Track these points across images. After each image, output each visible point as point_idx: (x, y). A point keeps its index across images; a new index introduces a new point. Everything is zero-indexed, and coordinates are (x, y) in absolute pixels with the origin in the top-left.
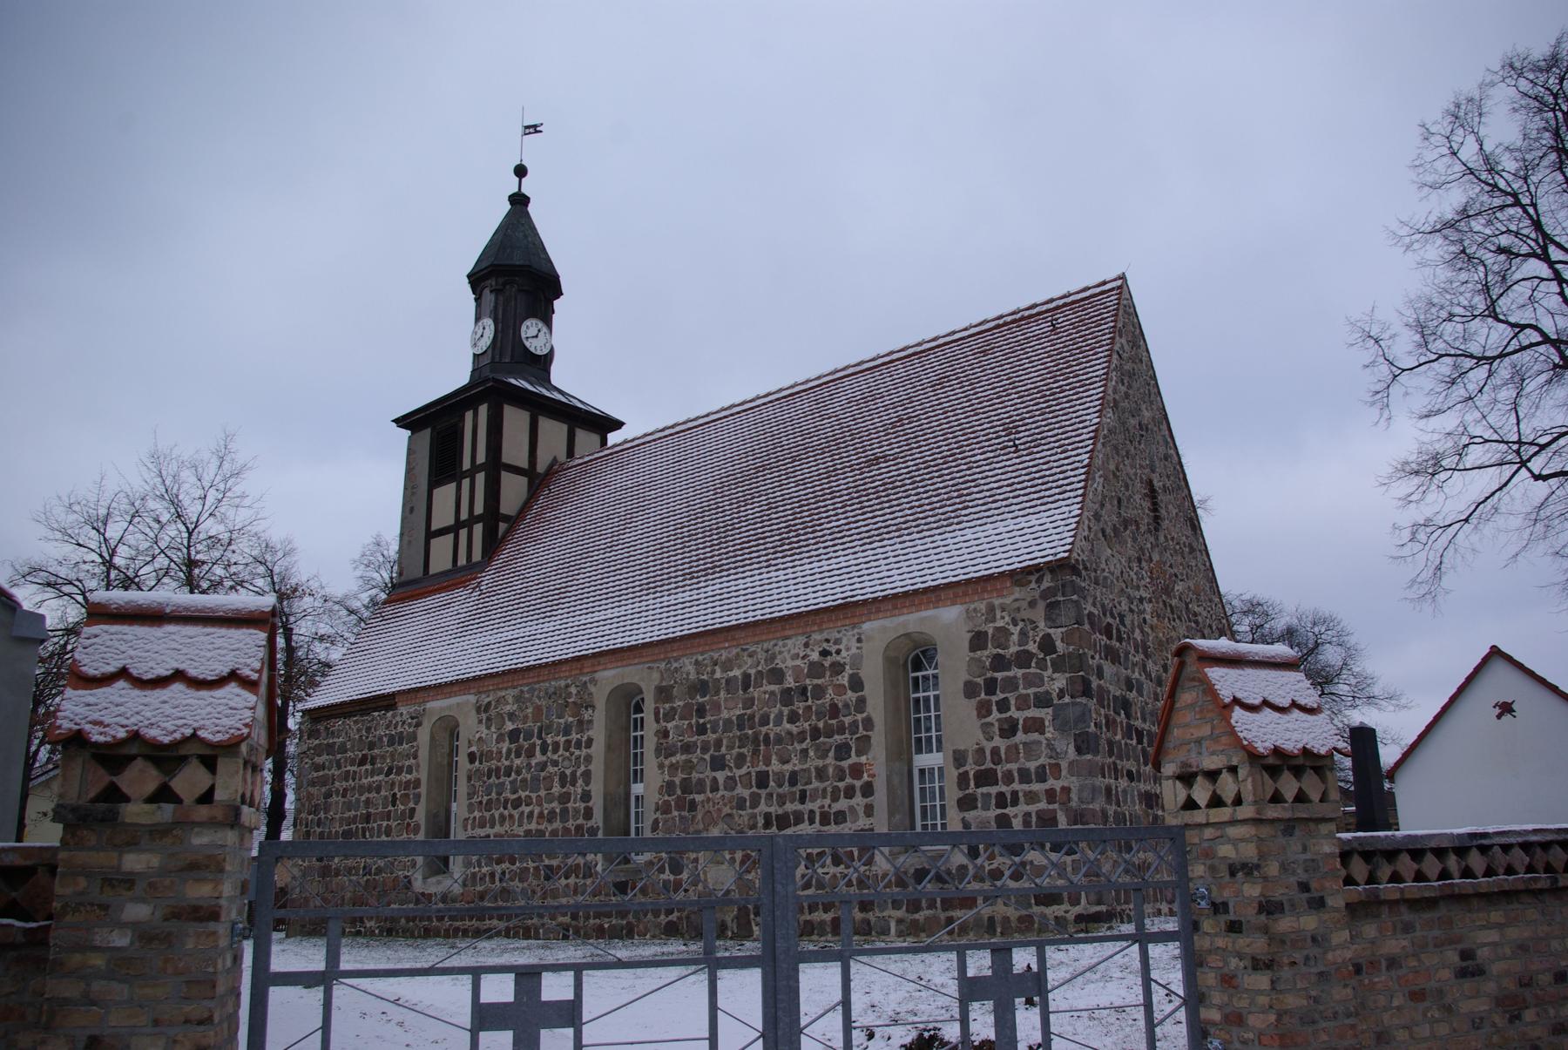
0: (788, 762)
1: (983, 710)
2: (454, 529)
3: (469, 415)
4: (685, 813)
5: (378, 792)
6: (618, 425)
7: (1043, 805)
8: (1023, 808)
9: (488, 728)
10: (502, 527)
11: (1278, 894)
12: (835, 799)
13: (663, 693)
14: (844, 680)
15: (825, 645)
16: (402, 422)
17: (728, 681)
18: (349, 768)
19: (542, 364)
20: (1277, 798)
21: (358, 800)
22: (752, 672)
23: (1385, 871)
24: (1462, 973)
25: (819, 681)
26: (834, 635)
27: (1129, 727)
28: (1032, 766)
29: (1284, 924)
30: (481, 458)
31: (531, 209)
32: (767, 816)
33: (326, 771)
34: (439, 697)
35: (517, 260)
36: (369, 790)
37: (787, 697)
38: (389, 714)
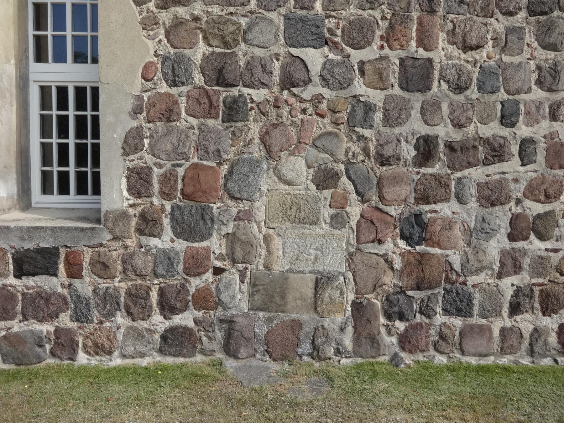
0: (478, 47)
4: (214, 123)
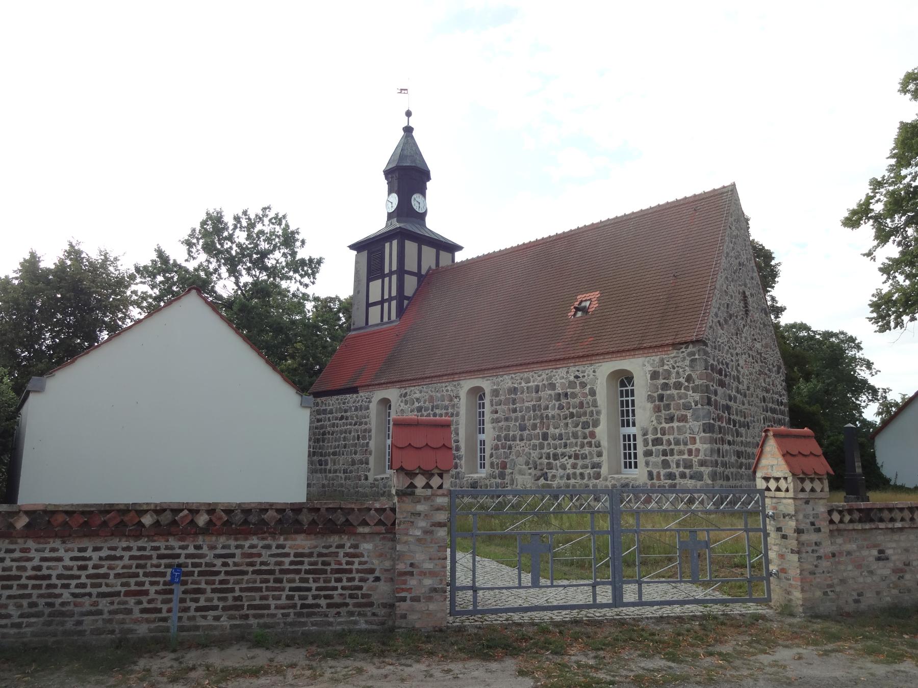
1: (657, 409)
2: (381, 302)
3: (387, 245)
5: (350, 434)
6: (459, 248)
7: (686, 456)
8: (676, 457)
9: (406, 404)
10: (406, 302)
11: (802, 526)
12: (582, 446)
13: (495, 393)
14: (587, 391)
15: (577, 373)
16: (352, 247)
17: (528, 388)
18: (334, 421)
19: (422, 216)
20: (803, 490)
21: (340, 437)
22: (540, 384)
23: (847, 518)
24: (879, 559)
25: (573, 390)
26: (581, 368)
27: (730, 419)
28: (681, 437)
29: (804, 537)
30: (394, 268)
31: (414, 134)
32: (548, 454)
33: (323, 423)
35: (407, 163)
36: (345, 432)
37: (558, 397)
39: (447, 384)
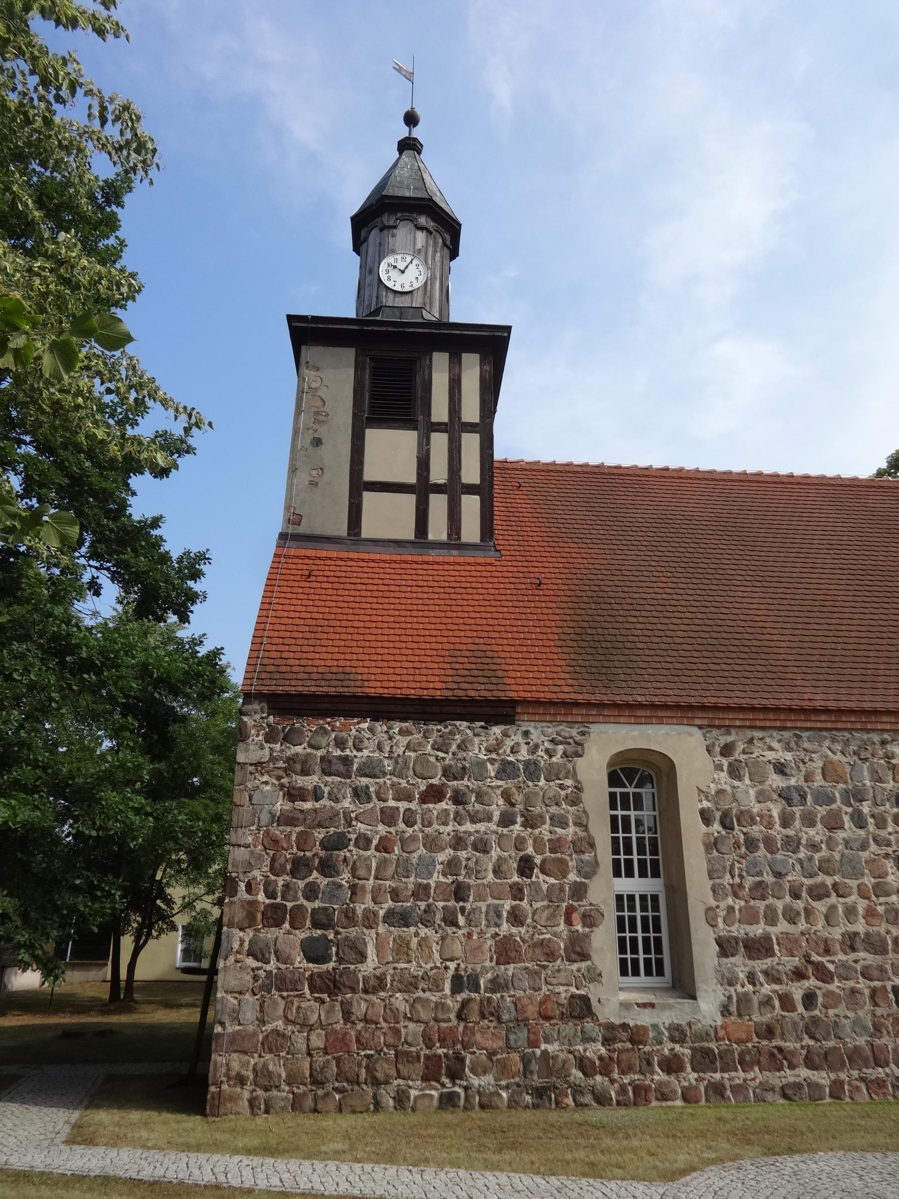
34: (622, 720)
38: (497, 730)
39: (886, 736)
